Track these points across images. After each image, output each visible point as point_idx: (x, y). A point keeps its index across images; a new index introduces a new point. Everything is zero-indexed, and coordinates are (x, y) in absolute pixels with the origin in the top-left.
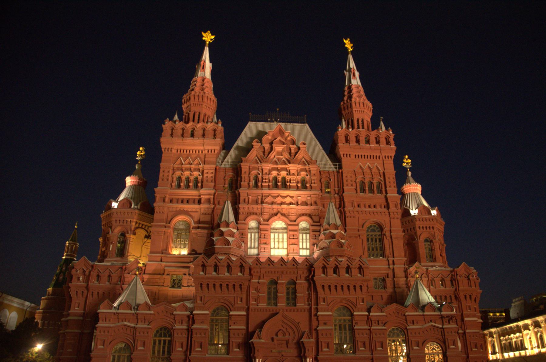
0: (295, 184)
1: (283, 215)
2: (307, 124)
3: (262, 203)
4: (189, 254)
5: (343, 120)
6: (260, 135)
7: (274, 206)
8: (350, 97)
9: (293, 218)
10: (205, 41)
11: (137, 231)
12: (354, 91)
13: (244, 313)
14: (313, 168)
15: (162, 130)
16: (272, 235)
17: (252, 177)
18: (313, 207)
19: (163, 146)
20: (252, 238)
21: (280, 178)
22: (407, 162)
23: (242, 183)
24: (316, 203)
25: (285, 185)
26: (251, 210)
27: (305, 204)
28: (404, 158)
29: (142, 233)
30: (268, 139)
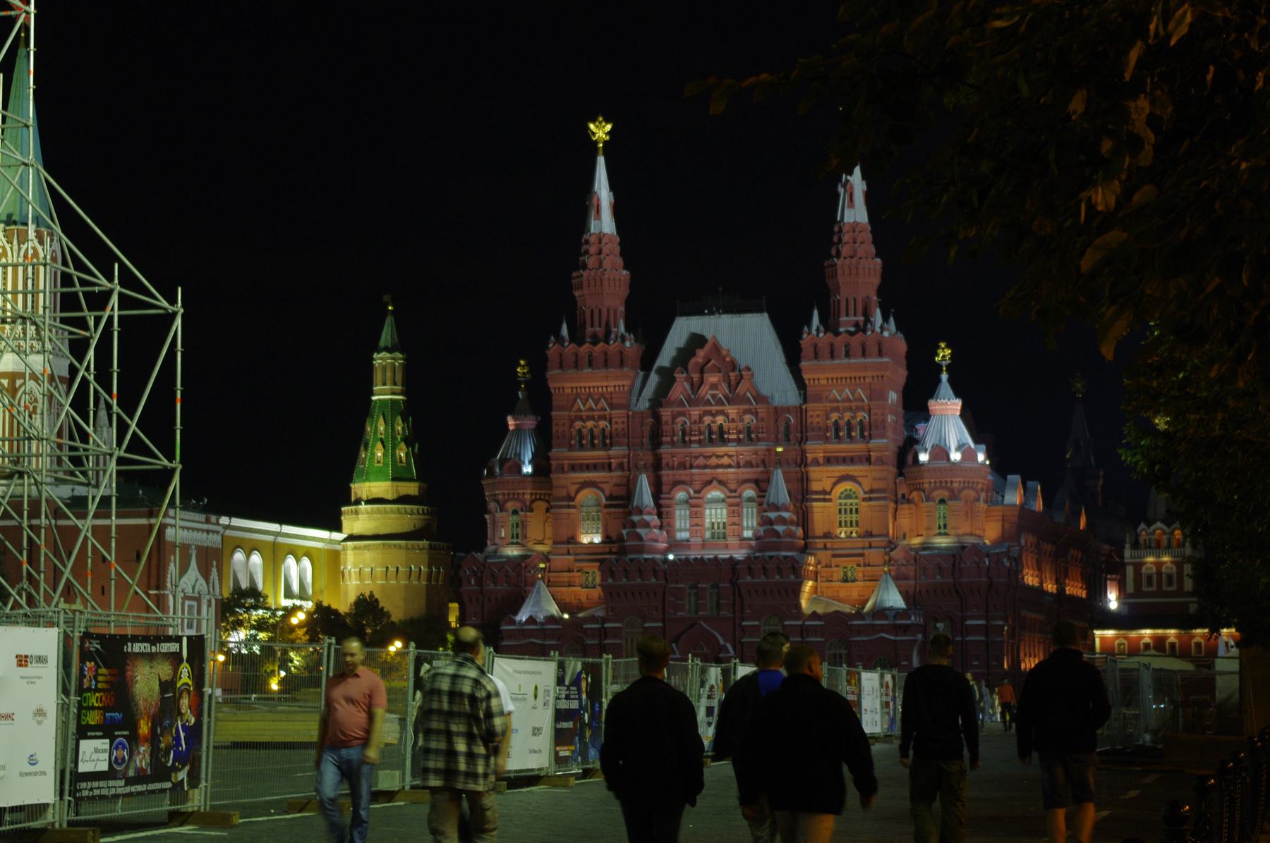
0: (735, 437)
1: (721, 483)
2: (766, 314)
3: (691, 467)
4: (603, 542)
5: (816, 313)
6: (697, 341)
7: (708, 471)
8: (838, 255)
9: (733, 486)
10: (596, 142)
11: (534, 505)
12: (846, 238)
13: (660, 624)
14: (762, 410)
15: (546, 358)
16: (707, 512)
17: (679, 427)
18: (761, 469)
19: (551, 385)
20: (681, 518)
21: (715, 427)
22: (944, 354)
23: (664, 439)
24: (763, 462)
25: (720, 437)
26: (677, 478)
27: (749, 464)
28: (939, 347)
29: (542, 505)
30: (696, 363)
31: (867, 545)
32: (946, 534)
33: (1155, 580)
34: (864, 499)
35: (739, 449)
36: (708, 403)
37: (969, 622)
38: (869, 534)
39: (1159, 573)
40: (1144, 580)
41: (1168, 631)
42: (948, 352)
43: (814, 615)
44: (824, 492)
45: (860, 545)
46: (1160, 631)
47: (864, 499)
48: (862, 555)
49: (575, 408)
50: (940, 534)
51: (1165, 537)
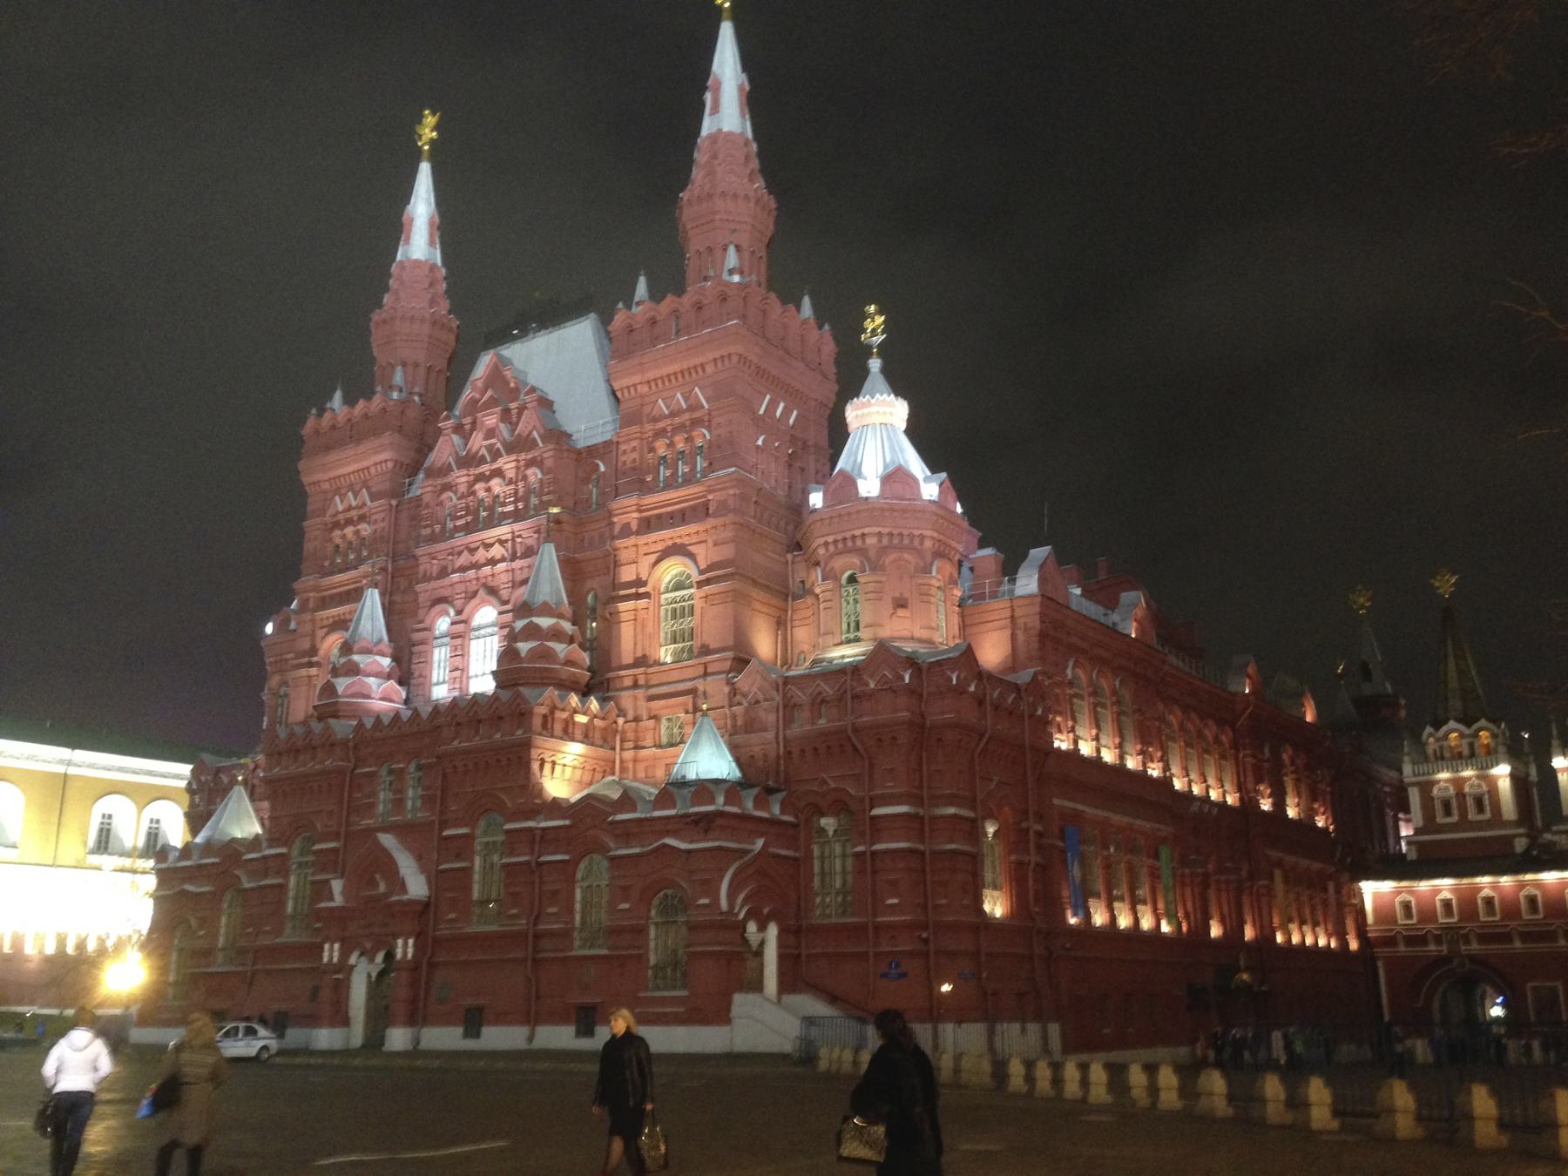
0: (511, 508)
1: (493, 591)
7: (471, 573)
19: (306, 479)
22: (875, 324)
28: (865, 316)
31: (701, 670)
32: (857, 640)
34: (700, 584)
35: (517, 527)
36: (482, 461)
37: (878, 811)
38: (705, 650)
39: (1461, 795)
40: (1438, 806)
41: (1479, 880)
42: (880, 320)
43: (556, 807)
44: (639, 582)
45: (689, 673)
46: (1465, 881)
47: (700, 584)
48: (693, 692)
49: (331, 511)
50: (849, 641)
51: (1465, 742)
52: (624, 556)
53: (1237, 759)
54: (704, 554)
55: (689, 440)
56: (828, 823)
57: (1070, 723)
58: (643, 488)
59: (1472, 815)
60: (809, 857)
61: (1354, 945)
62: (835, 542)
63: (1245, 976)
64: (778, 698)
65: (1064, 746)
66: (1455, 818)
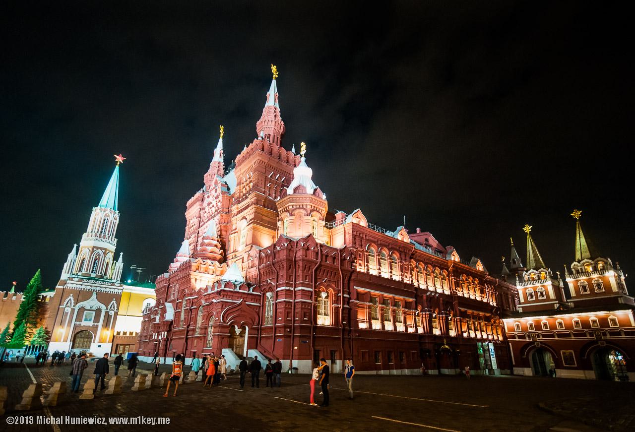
33: (534, 295)
39: (536, 292)
52: (234, 222)
53: (449, 280)
54: (250, 217)
55: (249, 187)
56: (269, 294)
57: (366, 264)
58: (239, 202)
59: (540, 298)
60: (264, 305)
61: (501, 338)
62: (282, 210)
63: (447, 347)
64: (258, 255)
65: (362, 271)
66: (534, 299)
